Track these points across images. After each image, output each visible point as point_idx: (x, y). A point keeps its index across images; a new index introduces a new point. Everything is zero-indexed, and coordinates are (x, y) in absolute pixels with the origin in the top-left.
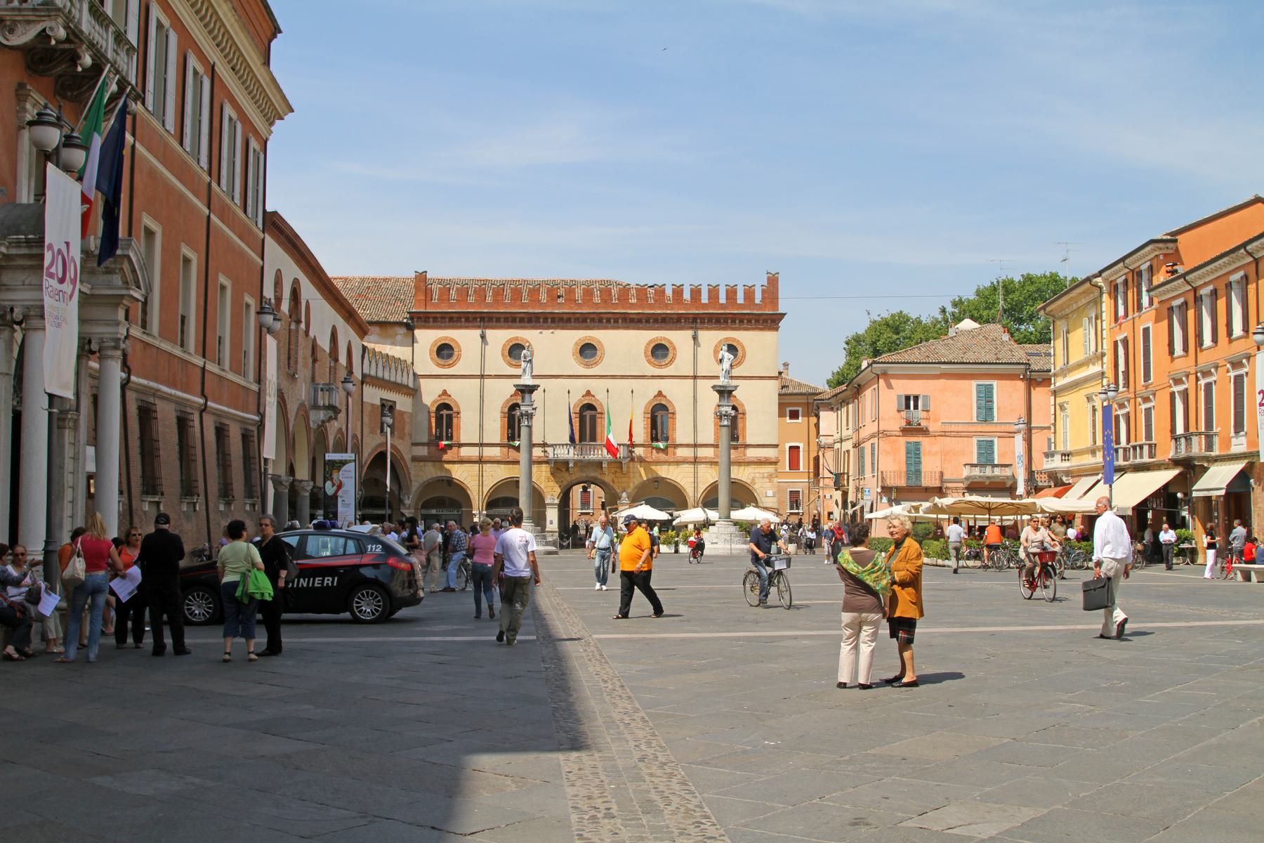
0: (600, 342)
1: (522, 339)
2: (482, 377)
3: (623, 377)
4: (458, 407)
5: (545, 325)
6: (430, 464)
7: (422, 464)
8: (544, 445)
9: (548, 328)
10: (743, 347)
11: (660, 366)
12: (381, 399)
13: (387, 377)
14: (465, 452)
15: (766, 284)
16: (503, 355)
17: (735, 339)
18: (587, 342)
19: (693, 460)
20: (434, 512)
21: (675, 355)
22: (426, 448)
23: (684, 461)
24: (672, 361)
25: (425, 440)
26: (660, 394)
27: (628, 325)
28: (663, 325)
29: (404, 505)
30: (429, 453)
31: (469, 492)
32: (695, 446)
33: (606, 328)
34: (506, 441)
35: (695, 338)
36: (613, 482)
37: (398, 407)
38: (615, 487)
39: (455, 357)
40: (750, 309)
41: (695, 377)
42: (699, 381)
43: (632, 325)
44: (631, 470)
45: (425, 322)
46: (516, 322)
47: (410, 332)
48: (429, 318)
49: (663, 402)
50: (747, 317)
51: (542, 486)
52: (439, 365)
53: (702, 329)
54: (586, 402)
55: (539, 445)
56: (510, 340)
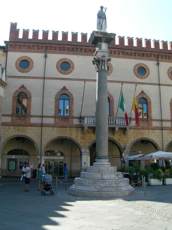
1: (68, 59)
4: (31, 95)
6: (12, 127)
7: (7, 127)
8: (81, 118)
9: (83, 55)
11: (142, 78)
14: (33, 120)
16: (57, 67)
19: (161, 129)
21: (149, 73)
22: (10, 118)
23: (156, 128)
24: (148, 76)
25: (10, 113)
26: (143, 92)
27: (125, 56)
28: (142, 57)
30: (12, 121)
31: (35, 144)
32: (162, 121)
35: (158, 64)
36: (119, 140)
38: (120, 143)
39: (30, 67)
45: (14, 48)
46: (65, 50)
47: (5, 53)
48: (16, 45)
49: (145, 97)
51: (79, 142)
52: (20, 71)
53: (161, 61)
55: (77, 118)
56: (62, 59)
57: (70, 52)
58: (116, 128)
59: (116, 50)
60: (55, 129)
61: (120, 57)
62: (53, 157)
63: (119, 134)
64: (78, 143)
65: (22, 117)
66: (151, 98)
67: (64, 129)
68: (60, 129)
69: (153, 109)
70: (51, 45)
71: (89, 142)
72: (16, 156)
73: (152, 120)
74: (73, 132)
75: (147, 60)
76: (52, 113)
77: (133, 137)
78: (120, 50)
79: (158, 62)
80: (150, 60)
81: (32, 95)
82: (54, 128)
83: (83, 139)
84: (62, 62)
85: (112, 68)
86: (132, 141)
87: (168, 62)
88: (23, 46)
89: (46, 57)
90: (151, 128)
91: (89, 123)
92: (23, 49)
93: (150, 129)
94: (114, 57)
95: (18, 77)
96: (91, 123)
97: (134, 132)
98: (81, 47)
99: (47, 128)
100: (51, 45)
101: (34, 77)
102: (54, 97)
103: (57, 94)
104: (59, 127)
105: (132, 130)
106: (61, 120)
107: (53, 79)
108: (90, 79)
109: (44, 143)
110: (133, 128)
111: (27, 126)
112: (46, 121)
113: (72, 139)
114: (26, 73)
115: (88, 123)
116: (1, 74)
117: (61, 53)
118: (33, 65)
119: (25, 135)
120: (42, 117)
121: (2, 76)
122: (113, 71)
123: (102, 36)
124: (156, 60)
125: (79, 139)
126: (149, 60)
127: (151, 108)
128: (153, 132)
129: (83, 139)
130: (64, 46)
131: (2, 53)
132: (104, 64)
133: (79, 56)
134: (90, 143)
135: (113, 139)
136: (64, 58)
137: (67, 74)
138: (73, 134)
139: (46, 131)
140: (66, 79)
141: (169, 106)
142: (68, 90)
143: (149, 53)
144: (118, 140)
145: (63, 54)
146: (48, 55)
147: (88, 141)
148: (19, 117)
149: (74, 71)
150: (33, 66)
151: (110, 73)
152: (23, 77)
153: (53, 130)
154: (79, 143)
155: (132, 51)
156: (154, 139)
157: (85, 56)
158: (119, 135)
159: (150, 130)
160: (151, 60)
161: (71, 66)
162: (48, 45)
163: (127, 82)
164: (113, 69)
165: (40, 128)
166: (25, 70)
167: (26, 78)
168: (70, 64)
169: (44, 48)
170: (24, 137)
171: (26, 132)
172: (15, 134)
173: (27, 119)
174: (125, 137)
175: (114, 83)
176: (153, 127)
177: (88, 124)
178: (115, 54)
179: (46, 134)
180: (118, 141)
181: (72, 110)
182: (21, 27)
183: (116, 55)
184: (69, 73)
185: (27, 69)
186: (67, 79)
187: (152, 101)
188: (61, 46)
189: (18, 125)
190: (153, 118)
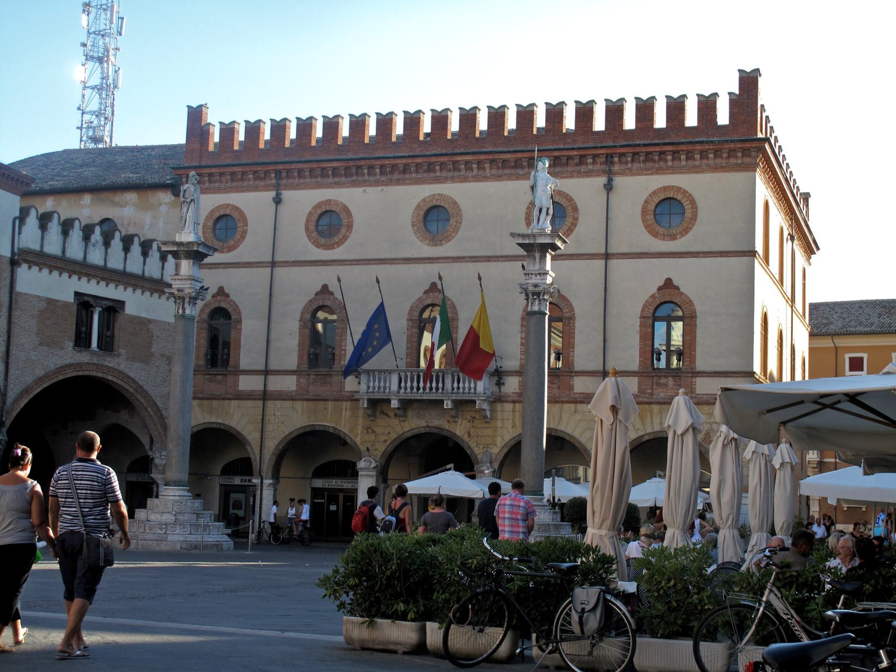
0: (455, 203)
1: (336, 203)
2: (273, 264)
3: (488, 259)
4: (239, 313)
5: (371, 178)
9: (377, 183)
10: (693, 202)
12: (77, 294)
13: (96, 257)
14: (246, 383)
15: (737, 93)
16: (307, 229)
17: (679, 189)
18: (435, 203)
20: (237, 481)
21: (576, 219)
29: (156, 466)
31: (248, 448)
33: (465, 180)
34: (305, 367)
35: (609, 187)
36: (469, 435)
37: (130, 310)
38: (472, 444)
40: (707, 135)
41: (607, 256)
42: (613, 263)
43: (507, 171)
44: (499, 417)
46: (328, 176)
50: (698, 147)
51: (358, 440)
53: (622, 173)
54: (429, 302)
56: (319, 205)
57: (343, 179)
58: (445, 402)
59: (469, 158)
60: (299, 405)
61: (485, 179)
62: (339, 481)
63: (469, 417)
64: (355, 443)
65: (218, 376)
66: (575, 303)
67: (322, 403)
68: (310, 403)
69: (579, 339)
70: (288, 167)
71: (385, 441)
72: (244, 478)
73: (573, 374)
74: (343, 414)
75: (572, 177)
76: (292, 362)
77: (511, 426)
78: (482, 157)
79: (610, 180)
80: (584, 176)
81: (242, 313)
82: (294, 402)
83: (368, 432)
84: (319, 212)
85: (461, 215)
86: (506, 441)
87: (646, 174)
88: (218, 174)
89: (278, 201)
90: (566, 399)
91: (371, 390)
92: (221, 182)
93: (563, 402)
94: (469, 181)
95: (209, 266)
96: (382, 389)
97: (514, 411)
98: (368, 162)
99: (278, 403)
100: (288, 167)
101: (247, 263)
102: (298, 317)
103: (304, 308)
104: (308, 400)
105: (509, 407)
106: (314, 379)
107: (295, 266)
108: (394, 257)
109: (272, 445)
110: (510, 399)
111: (229, 399)
112: (278, 384)
113: (342, 434)
114: (229, 252)
115: (369, 388)
116: (160, 264)
117: (319, 186)
118: (245, 228)
119: (226, 423)
120: (266, 372)
121: (163, 268)
122: (463, 226)
123: (175, 249)
124: (603, 172)
125: (359, 432)
126: (578, 177)
127: (574, 333)
128: (575, 412)
129: (368, 432)
130: (324, 165)
131: (171, 198)
132: (183, 304)
133: (370, 190)
134: (387, 444)
135: (451, 432)
136: (327, 201)
137: (334, 248)
138: (343, 419)
139: (277, 413)
140: (330, 263)
141: (638, 324)
142: (334, 295)
143: (575, 153)
144: (467, 434)
145: (325, 188)
146: (286, 194)
147: (383, 438)
148: (210, 374)
149: (355, 237)
150: (247, 230)
151: (453, 234)
152: (222, 266)
153: (293, 408)
154: (359, 444)
155: (519, 155)
156: (577, 434)
157: (385, 188)
158: (469, 422)
159: (567, 406)
160: (588, 174)
161: (345, 221)
162: (280, 167)
163: (502, 257)
164: (461, 219)
165: (261, 403)
166: (225, 245)
167: (230, 267)
168: (343, 215)
169: (273, 175)
170: (222, 427)
171: (227, 414)
172: (201, 421)
173: (230, 379)
174: (486, 426)
175: (462, 264)
176: (576, 396)
177: (367, 392)
178: (471, 169)
179: (277, 418)
180: (466, 438)
181: (343, 352)
182: (215, 118)
183: (475, 172)
184: (339, 244)
185: (232, 243)
186: (334, 263)
187: (577, 311)
188: (315, 165)
189: (208, 396)
190: (578, 367)
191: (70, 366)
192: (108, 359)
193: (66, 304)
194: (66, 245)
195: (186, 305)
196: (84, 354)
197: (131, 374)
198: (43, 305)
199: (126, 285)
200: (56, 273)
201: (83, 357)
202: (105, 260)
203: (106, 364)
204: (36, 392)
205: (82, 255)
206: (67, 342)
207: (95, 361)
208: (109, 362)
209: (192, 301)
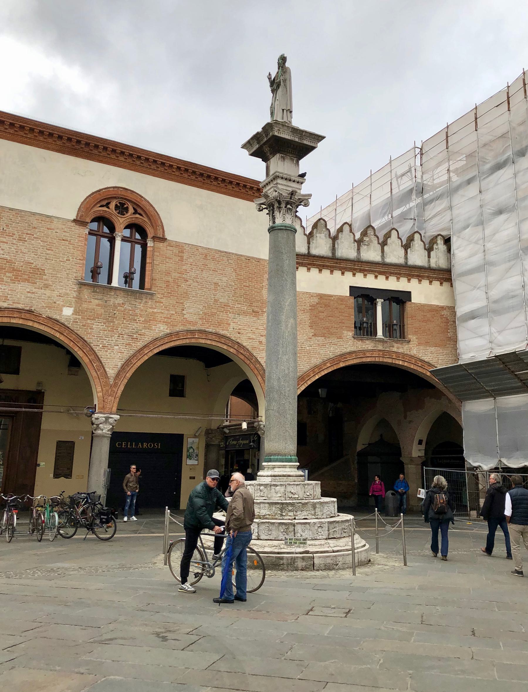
37: (416, 299)
132: (273, 213)
191: (350, 353)
192: (396, 345)
193: (341, 299)
194: (336, 246)
195: (277, 213)
196: (367, 342)
197: (426, 359)
198: (316, 300)
199: (410, 277)
200: (326, 272)
201: (368, 345)
202: (383, 256)
203: (395, 349)
204: (313, 379)
205: (356, 254)
206: (345, 332)
207: (380, 347)
208: (398, 348)
209: (283, 205)
